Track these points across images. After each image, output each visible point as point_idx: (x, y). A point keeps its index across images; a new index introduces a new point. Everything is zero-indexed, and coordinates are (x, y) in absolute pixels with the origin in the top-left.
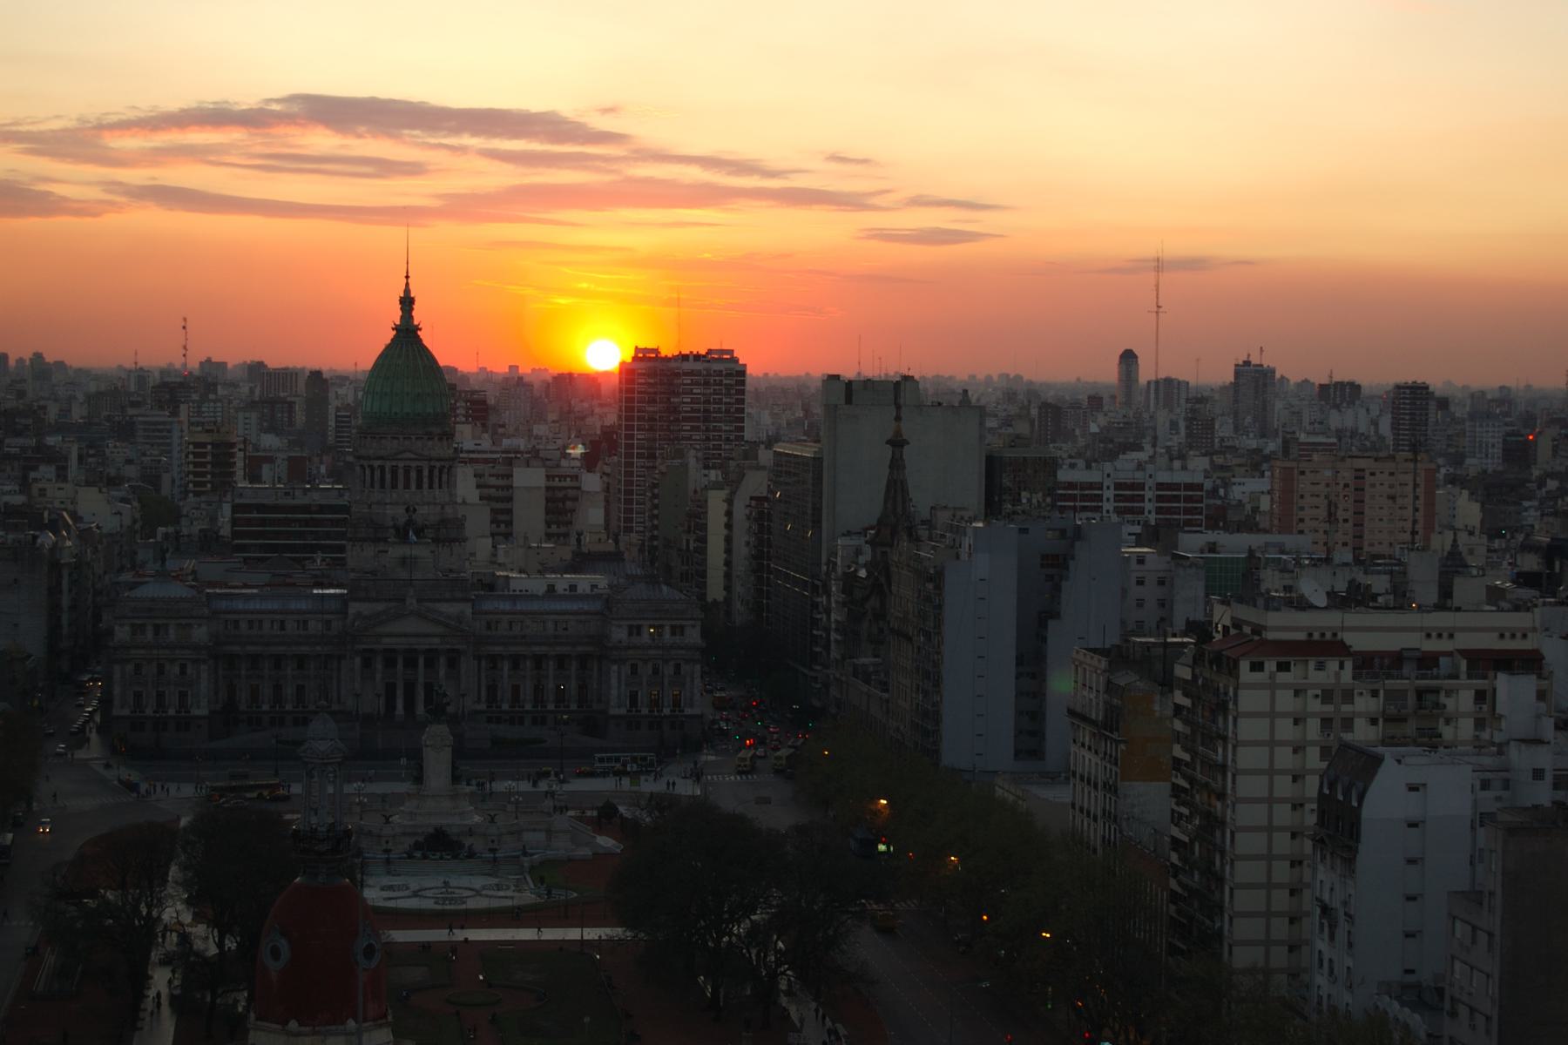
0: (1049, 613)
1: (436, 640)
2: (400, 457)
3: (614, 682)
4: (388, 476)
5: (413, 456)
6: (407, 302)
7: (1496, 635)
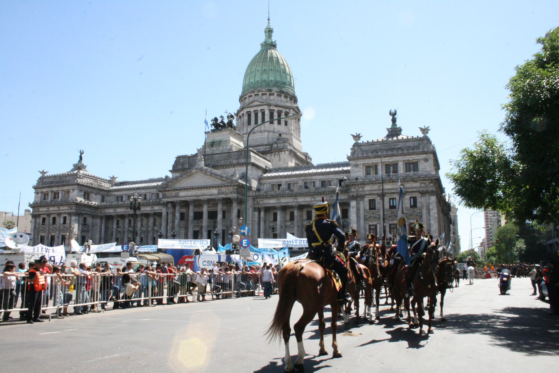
1: (215, 191)
5: (258, 103)
6: (269, 32)
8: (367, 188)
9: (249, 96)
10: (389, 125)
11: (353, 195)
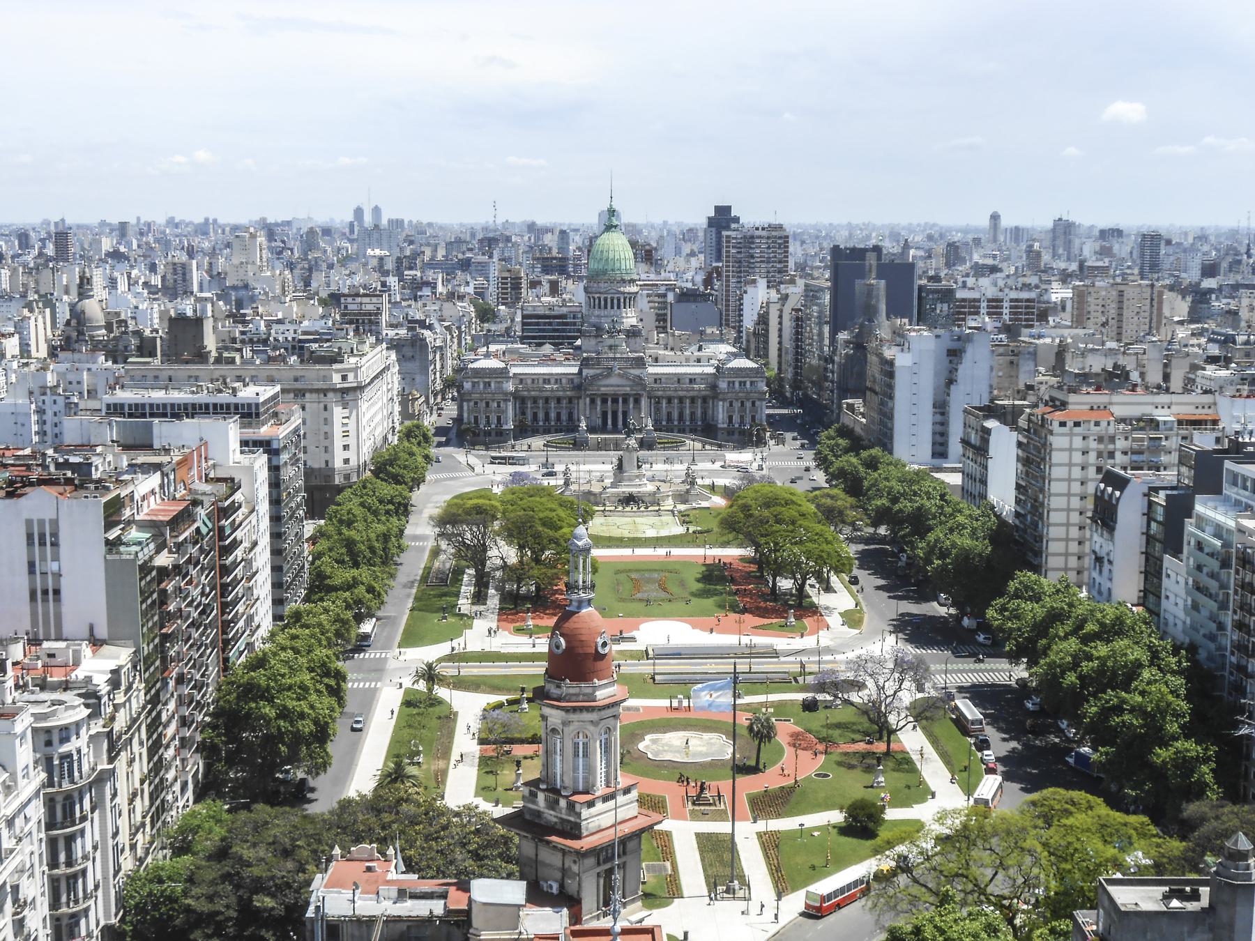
0: (951, 382)
1: (628, 389)
3: (721, 410)
4: (603, 303)
7: (1194, 407)
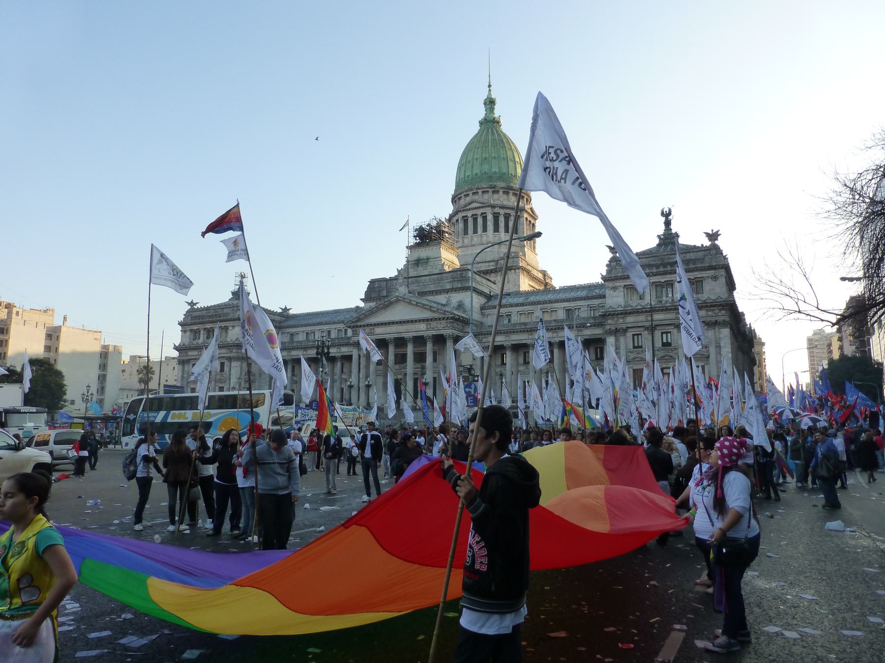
1: (422, 326)
2: (468, 207)
5: (478, 205)
6: (490, 103)
8: (630, 319)
9: (465, 195)
10: (661, 229)
11: (610, 329)
